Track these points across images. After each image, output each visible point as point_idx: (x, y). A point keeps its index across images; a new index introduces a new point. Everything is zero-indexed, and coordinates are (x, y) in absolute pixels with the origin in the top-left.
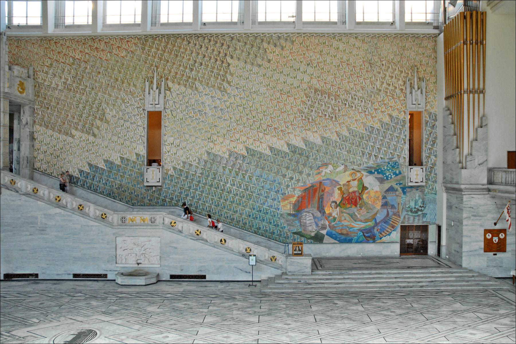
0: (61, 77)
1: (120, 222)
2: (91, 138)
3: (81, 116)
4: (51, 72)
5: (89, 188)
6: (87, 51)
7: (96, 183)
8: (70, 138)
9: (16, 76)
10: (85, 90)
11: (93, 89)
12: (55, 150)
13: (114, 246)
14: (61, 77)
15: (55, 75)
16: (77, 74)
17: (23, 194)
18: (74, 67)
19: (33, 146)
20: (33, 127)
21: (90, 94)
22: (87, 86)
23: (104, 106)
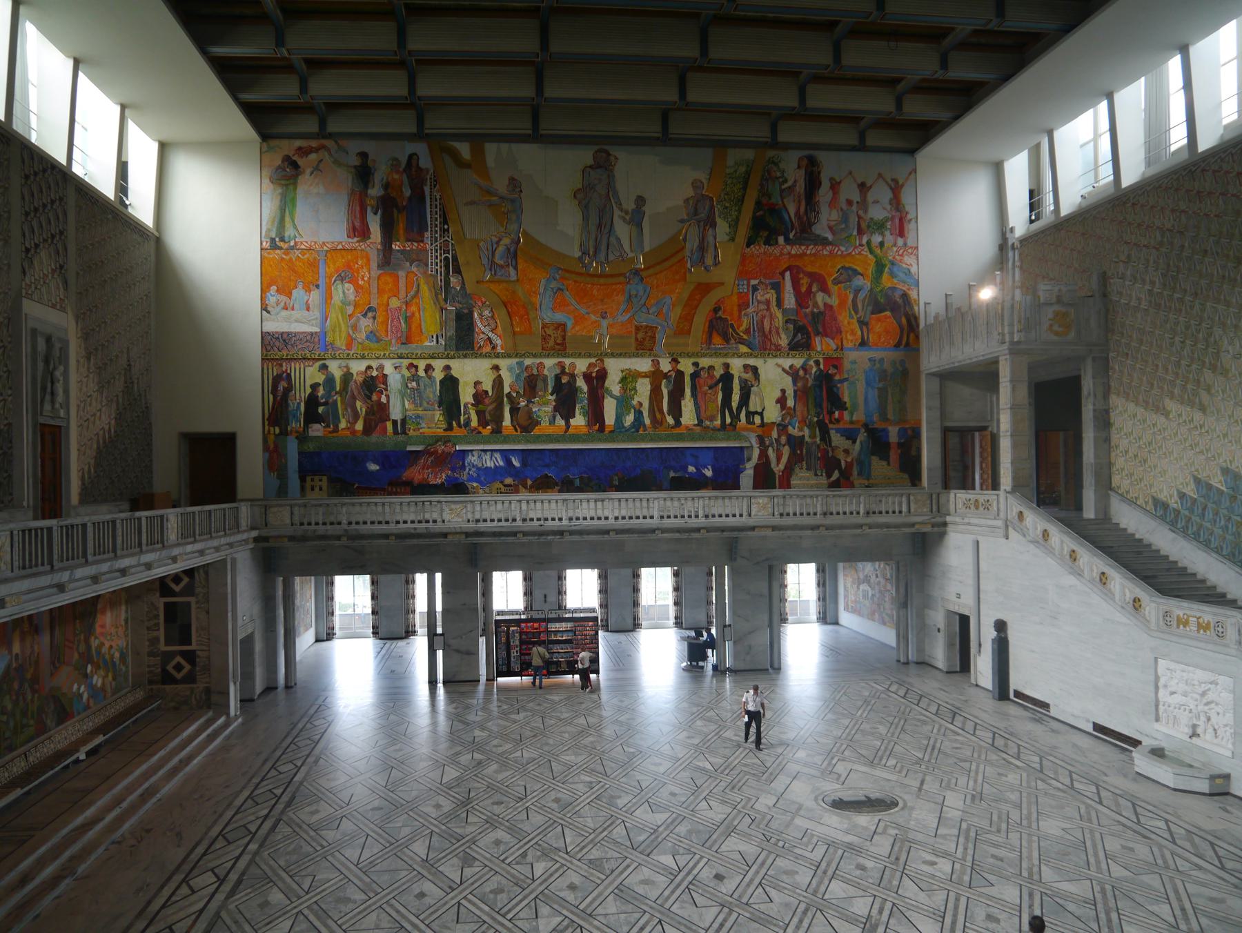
0: (1144, 281)
1: (1162, 623)
2: (1198, 416)
3: (1178, 364)
4: (1129, 273)
5: (1196, 537)
6: (1183, 206)
7: (1208, 525)
8: (1163, 419)
9: (1046, 304)
10: (1181, 300)
11: (1196, 294)
12: (1139, 447)
13: (1152, 678)
14: (1144, 281)
15: (1135, 278)
16: (1169, 265)
17: (1031, 542)
18: (1163, 250)
19: (1107, 440)
20: (1106, 396)
21: (1192, 307)
22: (1185, 291)
23: (1218, 331)
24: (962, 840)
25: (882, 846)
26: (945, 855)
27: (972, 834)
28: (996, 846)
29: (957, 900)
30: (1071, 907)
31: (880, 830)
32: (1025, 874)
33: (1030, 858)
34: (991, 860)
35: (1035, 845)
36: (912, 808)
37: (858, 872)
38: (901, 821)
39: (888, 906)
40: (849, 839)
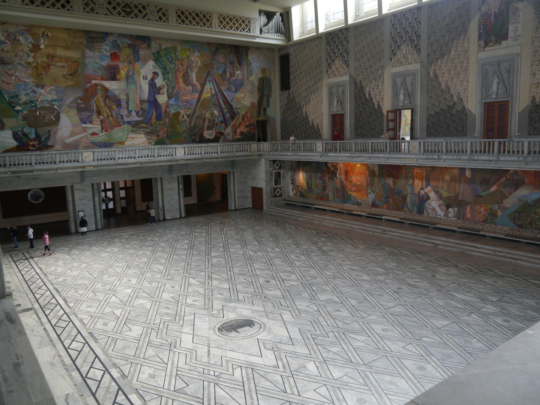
24: (183, 314)
25: (217, 305)
26: (189, 306)
27: (177, 318)
28: (167, 314)
29: (184, 290)
30: (145, 295)
31: (221, 311)
32: (158, 304)
33: (154, 310)
34: (170, 307)
35: (149, 318)
36: (210, 329)
37: (221, 292)
38: (213, 319)
39: (207, 284)
40: (233, 305)
